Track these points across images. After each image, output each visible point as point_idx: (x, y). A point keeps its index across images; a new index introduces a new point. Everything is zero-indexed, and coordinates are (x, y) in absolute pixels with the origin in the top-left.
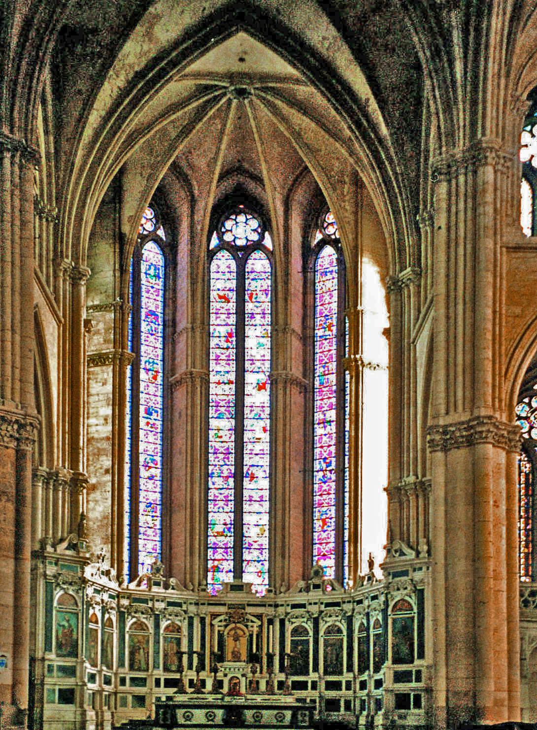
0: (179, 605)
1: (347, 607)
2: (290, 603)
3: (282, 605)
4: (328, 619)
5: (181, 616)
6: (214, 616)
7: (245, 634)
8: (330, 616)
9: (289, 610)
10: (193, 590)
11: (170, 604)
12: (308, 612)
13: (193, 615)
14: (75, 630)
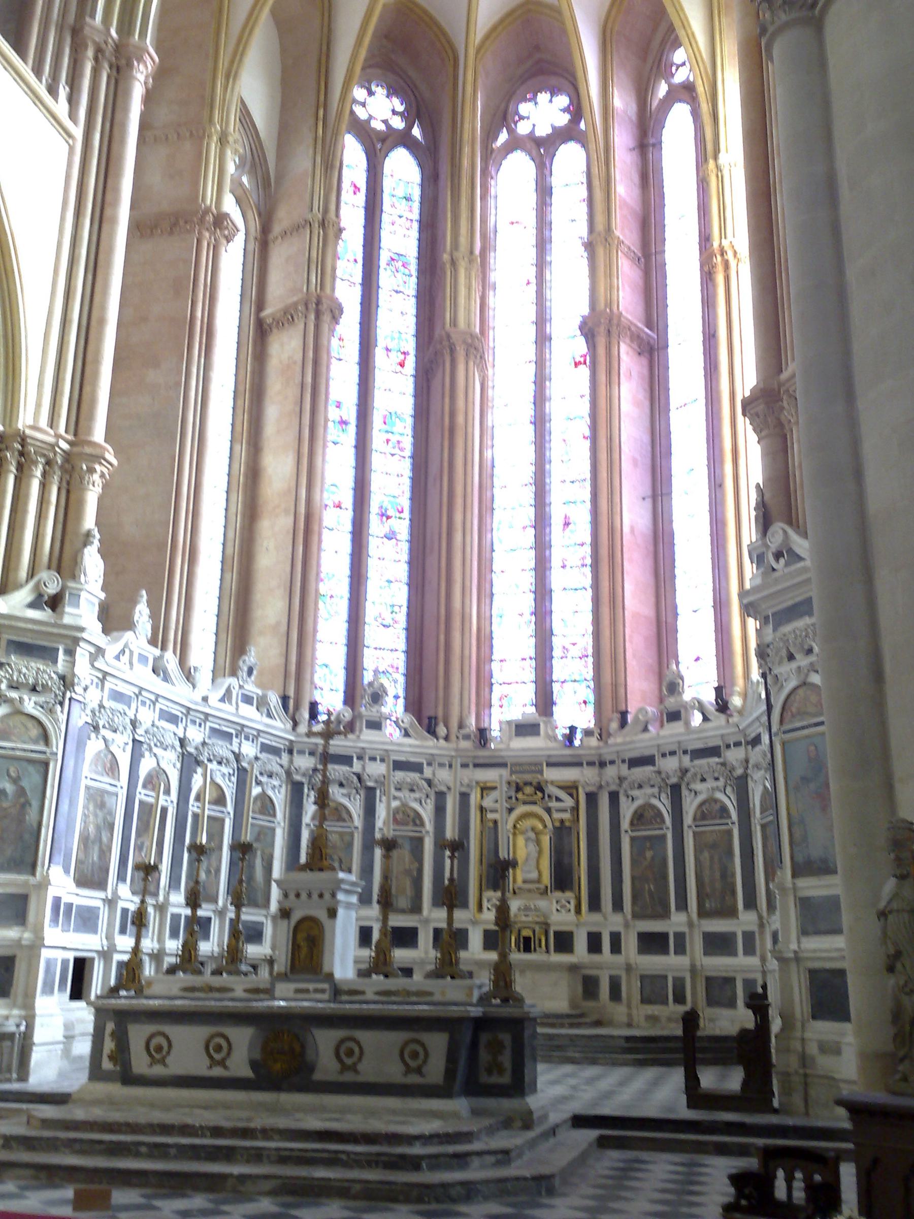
0: (417, 768)
1: (734, 756)
2: (627, 756)
3: (612, 762)
4: (698, 786)
5: (420, 789)
6: (486, 789)
7: (545, 826)
8: (703, 780)
9: (624, 770)
10: (447, 738)
11: (399, 766)
12: (659, 772)
13: (444, 789)
14: (35, 804)
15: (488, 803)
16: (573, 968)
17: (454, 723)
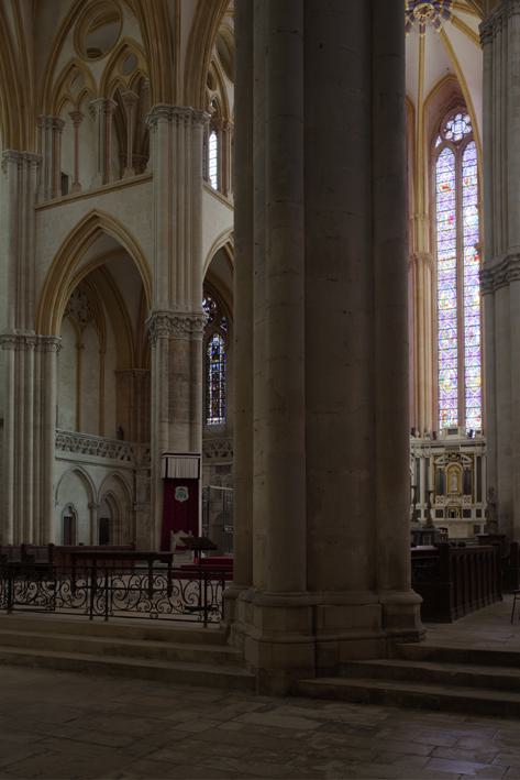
6: (436, 456)
15: (437, 461)
16: (469, 523)
17: (422, 431)
